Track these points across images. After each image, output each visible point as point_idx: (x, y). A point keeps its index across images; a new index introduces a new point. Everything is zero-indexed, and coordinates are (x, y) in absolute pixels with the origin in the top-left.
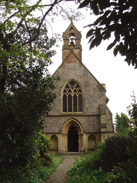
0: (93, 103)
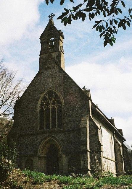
0: (74, 115)
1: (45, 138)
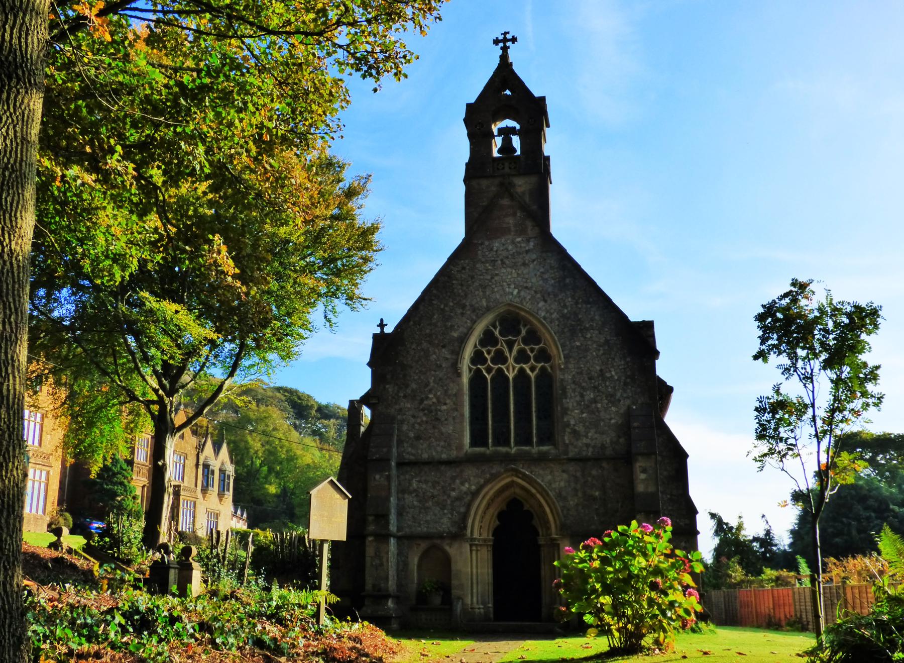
0: (599, 405)
1: (494, 477)
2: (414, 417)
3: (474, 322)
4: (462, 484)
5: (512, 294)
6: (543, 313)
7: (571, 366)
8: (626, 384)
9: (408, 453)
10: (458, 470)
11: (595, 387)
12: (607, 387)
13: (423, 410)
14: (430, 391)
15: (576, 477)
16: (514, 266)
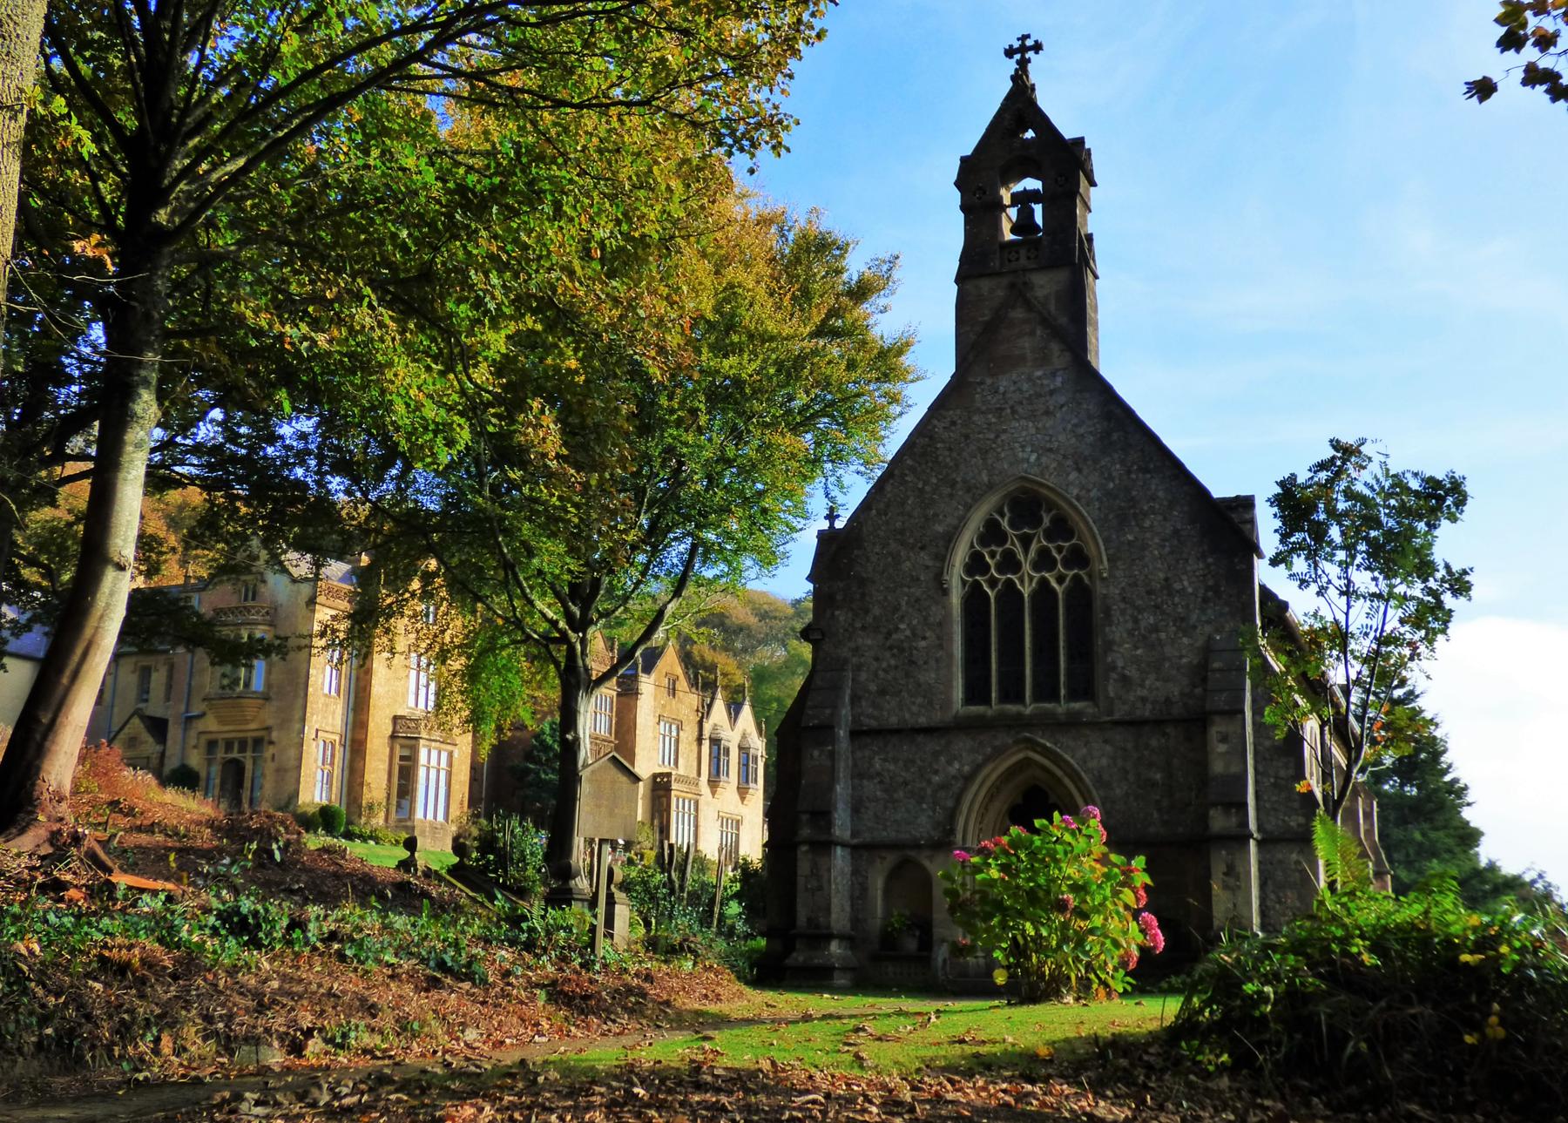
0: (1163, 635)
1: (999, 752)
2: (877, 659)
3: (968, 508)
4: (950, 763)
5: (1028, 460)
6: (1075, 489)
7: (1118, 573)
8: (1205, 600)
9: (868, 716)
10: (943, 742)
11: (1157, 607)
12: (1175, 605)
13: (891, 648)
14: (902, 619)
15: (1125, 750)
16: (1032, 416)
